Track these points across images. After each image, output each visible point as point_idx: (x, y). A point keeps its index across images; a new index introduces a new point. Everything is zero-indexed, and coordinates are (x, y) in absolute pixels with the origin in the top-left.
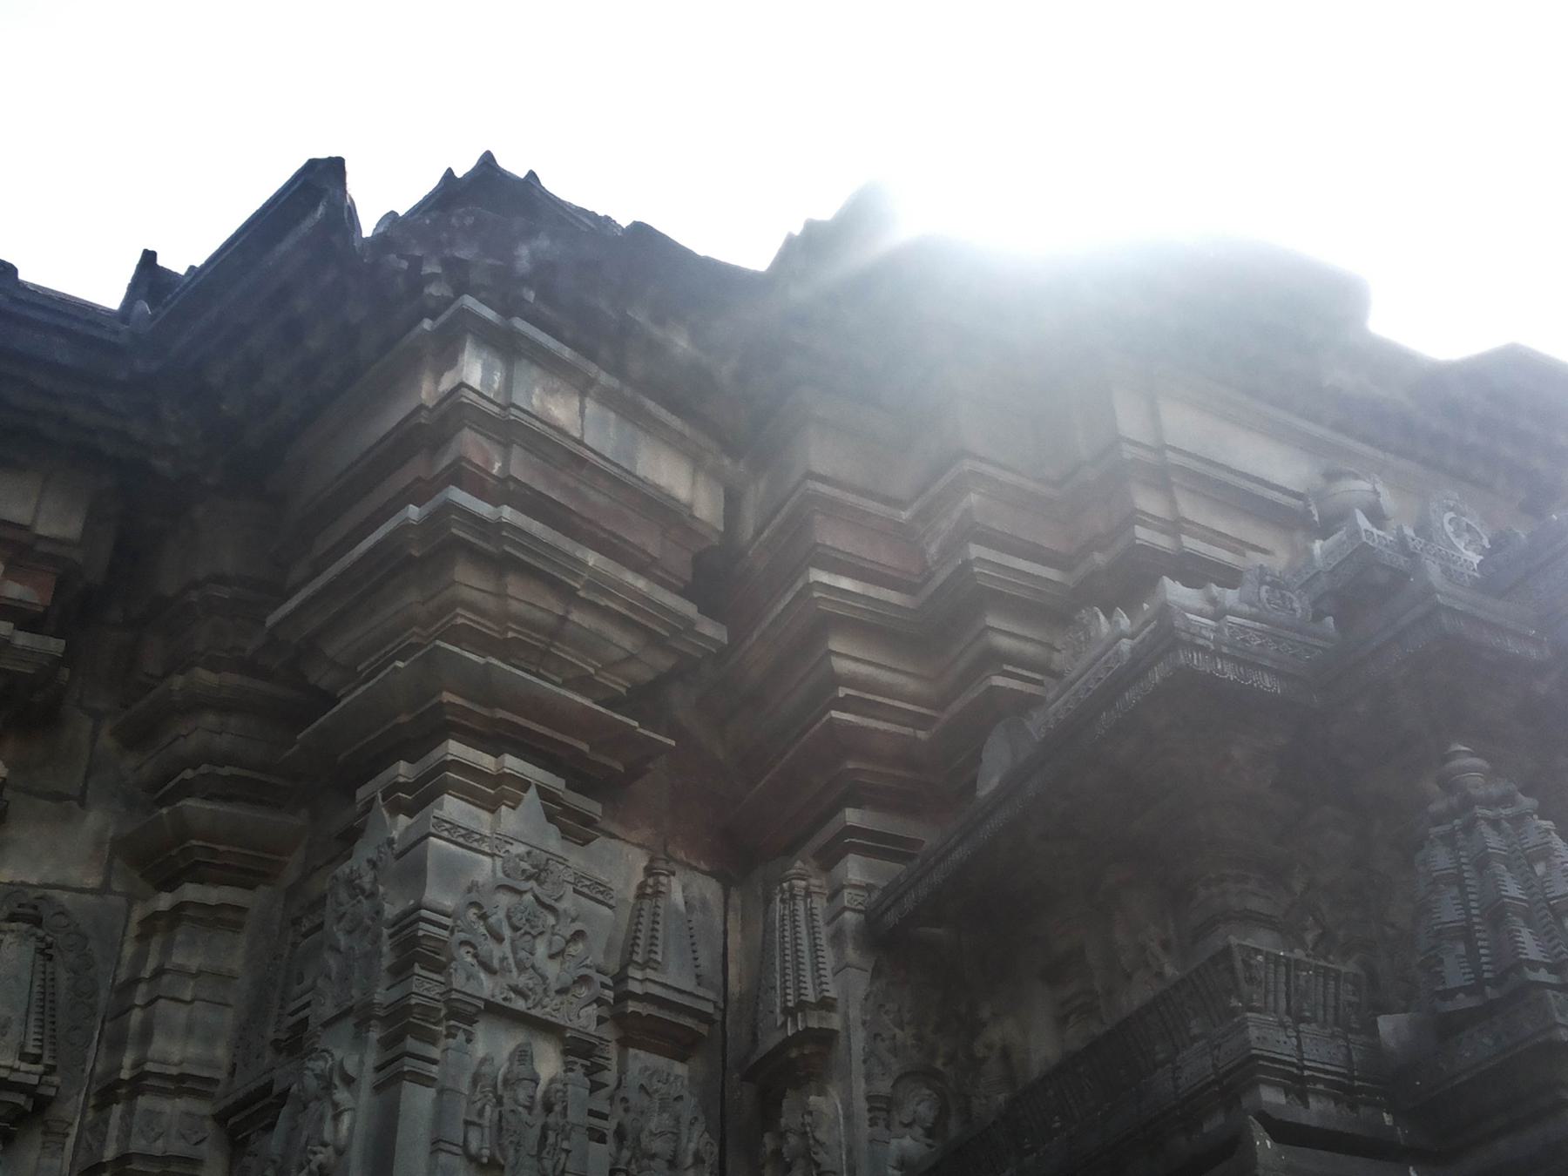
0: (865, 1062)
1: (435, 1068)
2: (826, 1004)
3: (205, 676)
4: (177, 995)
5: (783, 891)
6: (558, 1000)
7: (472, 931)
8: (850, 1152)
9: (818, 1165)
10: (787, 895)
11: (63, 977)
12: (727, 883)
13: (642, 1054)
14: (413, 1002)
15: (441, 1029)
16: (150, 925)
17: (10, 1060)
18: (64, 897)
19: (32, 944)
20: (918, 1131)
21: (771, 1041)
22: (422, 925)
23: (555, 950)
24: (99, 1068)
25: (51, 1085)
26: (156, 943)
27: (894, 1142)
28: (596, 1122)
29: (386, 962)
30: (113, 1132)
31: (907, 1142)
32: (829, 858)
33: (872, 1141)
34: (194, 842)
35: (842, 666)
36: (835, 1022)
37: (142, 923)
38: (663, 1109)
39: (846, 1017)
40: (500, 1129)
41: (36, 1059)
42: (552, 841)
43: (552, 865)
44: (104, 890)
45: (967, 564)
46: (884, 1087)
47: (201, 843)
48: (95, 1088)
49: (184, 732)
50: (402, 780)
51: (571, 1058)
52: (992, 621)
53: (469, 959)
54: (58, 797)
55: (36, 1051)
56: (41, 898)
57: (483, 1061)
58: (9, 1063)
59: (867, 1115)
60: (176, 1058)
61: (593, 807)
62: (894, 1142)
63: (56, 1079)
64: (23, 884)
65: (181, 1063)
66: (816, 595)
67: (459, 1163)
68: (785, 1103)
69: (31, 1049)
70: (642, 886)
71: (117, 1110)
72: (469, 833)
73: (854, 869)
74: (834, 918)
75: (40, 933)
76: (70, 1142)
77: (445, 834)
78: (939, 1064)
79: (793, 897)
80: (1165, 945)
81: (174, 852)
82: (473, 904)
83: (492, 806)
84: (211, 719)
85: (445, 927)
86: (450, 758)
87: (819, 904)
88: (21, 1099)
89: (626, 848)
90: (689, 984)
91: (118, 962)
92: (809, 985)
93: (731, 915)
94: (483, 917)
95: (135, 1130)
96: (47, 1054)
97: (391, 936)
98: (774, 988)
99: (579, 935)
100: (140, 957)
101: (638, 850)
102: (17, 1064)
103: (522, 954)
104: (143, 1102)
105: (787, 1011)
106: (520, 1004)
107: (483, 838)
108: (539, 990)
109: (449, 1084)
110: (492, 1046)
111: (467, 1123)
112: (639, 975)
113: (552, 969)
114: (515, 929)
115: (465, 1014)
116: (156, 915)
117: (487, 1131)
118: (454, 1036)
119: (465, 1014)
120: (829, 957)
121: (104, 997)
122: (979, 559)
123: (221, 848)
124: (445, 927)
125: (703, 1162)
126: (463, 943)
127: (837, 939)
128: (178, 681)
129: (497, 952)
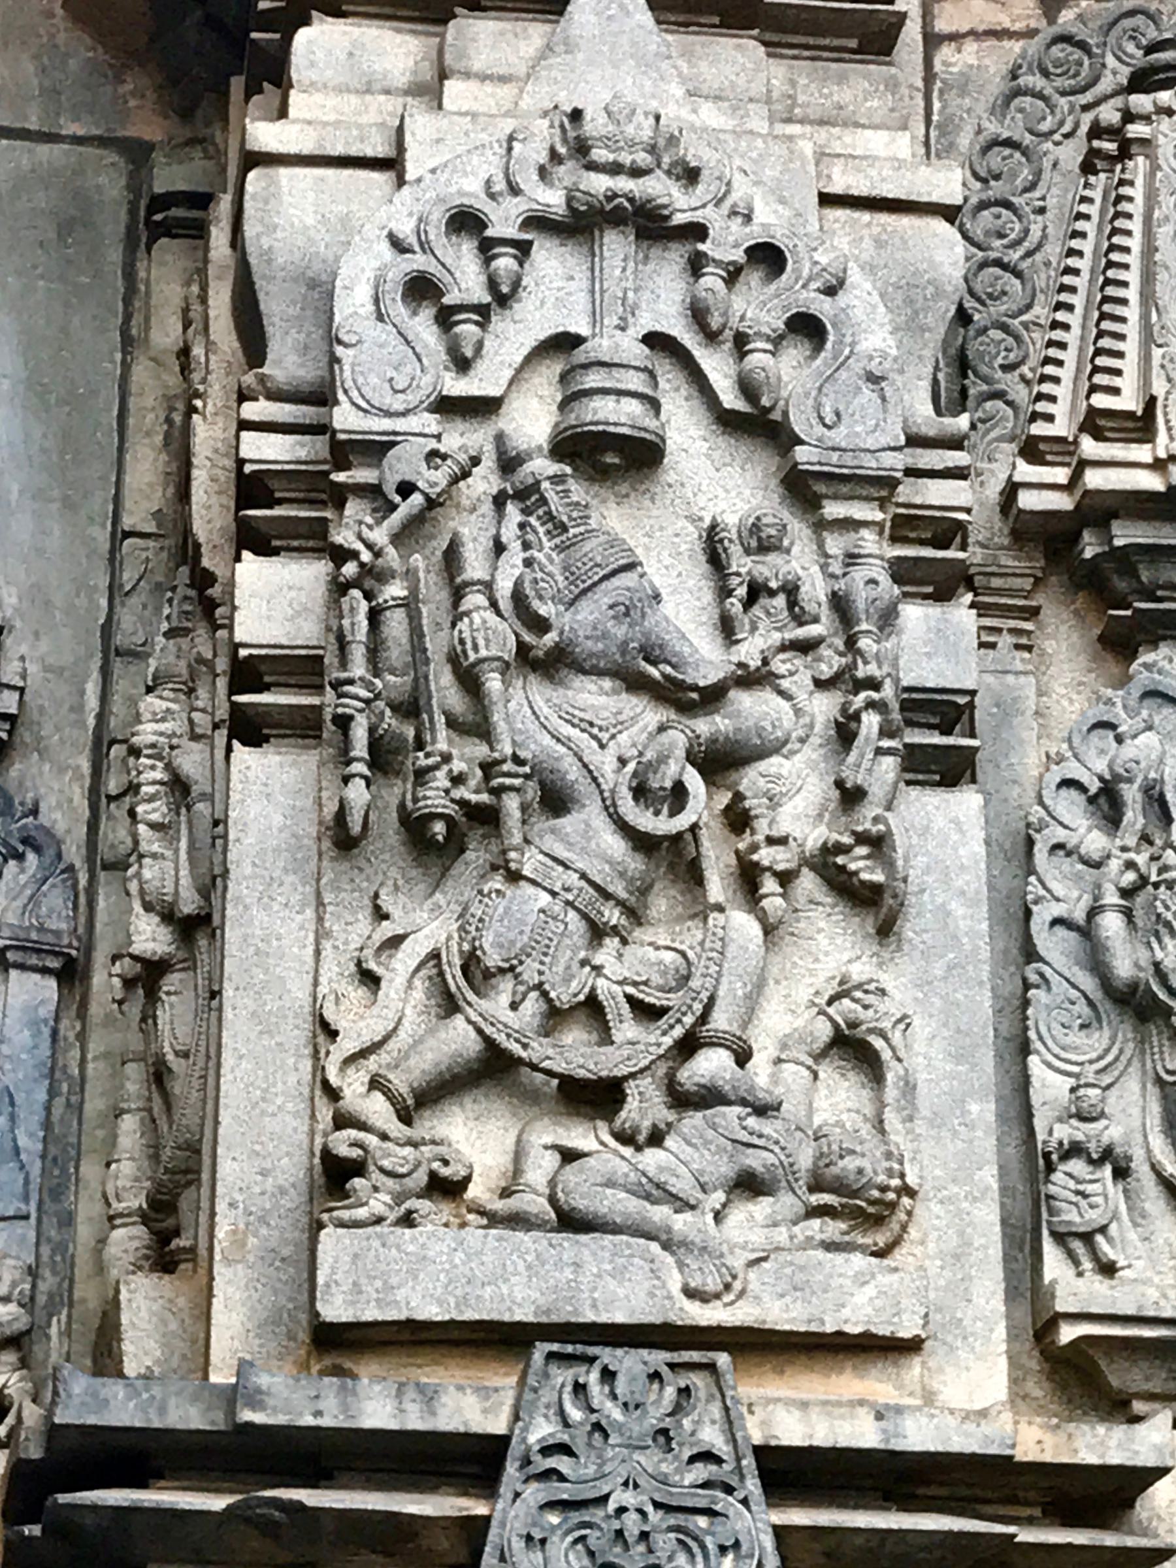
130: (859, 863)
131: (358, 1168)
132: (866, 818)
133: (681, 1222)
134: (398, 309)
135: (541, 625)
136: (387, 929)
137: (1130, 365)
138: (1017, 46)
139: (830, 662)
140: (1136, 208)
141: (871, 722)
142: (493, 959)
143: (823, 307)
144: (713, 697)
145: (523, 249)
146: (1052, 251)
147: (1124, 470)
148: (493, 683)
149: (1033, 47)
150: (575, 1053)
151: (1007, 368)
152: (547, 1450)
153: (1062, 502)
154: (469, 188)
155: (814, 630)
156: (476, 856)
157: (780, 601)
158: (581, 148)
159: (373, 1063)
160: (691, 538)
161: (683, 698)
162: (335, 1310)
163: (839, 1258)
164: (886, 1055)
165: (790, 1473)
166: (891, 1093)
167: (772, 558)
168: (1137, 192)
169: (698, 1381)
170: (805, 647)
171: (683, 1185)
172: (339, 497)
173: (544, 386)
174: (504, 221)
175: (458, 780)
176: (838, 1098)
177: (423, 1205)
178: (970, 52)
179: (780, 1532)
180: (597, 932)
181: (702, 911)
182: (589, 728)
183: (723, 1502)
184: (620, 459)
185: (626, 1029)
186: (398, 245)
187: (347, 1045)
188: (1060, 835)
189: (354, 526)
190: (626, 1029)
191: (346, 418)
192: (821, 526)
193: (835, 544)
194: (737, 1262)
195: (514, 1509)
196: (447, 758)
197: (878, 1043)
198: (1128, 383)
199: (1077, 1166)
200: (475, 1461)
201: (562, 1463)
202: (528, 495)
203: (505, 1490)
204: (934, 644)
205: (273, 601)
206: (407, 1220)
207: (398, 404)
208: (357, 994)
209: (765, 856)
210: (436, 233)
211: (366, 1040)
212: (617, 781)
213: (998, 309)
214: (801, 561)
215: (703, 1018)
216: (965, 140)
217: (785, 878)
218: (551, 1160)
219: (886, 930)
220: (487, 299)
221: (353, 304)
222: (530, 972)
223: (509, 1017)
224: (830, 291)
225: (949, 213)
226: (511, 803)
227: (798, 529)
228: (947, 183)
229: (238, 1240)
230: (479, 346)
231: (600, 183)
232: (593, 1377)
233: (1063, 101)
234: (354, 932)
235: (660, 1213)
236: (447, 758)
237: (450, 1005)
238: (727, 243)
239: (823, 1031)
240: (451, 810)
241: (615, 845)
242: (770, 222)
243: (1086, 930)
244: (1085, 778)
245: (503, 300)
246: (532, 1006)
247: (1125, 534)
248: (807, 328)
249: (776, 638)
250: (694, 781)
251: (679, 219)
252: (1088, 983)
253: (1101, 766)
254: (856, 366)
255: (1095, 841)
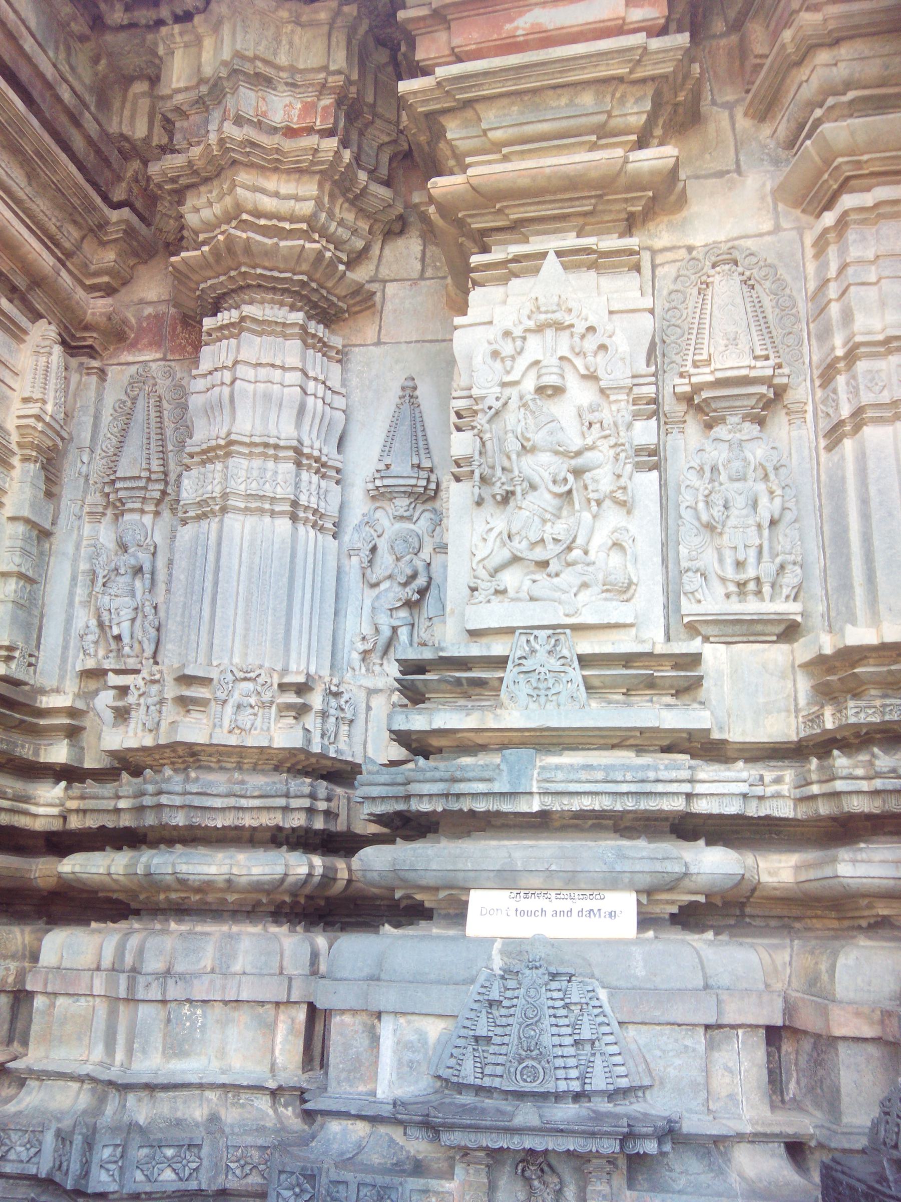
3: (808, 19)
4: (864, 280)
11: (767, 302)
16: (821, 244)
17: (748, 361)
18: (749, 243)
19: (737, 278)
24: (815, 358)
25: (783, 375)
26: (832, 252)
30: (843, 395)
34: (840, 160)
37: (815, 244)
41: (767, 358)
44: (777, 229)
47: (846, 159)
48: (816, 373)
49: (804, 78)
54: (721, 174)
55: (764, 353)
56: (732, 248)
58: (746, 363)
60: (878, 326)
63: (786, 370)
64: (714, 242)
65: (883, 330)
69: (759, 352)
71: (841, 380)
75: (740, 269)
76: (809, 416)
81: (826, 176)
84: (823, 56)
88: (763, 389)
91: (805, 279)
95: (862, 387)
96: (772, 356)
100: (823, 266)
102: (753, 363)
104: (861, 366)
116: (826, 231)
121: (803, 307)
123: (865, 157)
128: (787, 35)
130: (619, 495)
131: (476, 589)
132: (622, 482)
133: (564, 597)
134: (489, 360)
135: (528, 440)
136: (489, 526)
137: (705, 347)
138: (678, 264)
139: (612, 441)
140: (709, 302)
141: (623, 455)
142: (514, 531)
143: (607, 342)
144: (578, 454)
145: (524, 338)
146: (690, 319)
147: (704, 376)
148: (514, 457)
149: (683, 263)
150: (539, 554)
151: (677, 354)
152: (520, 658)
153: (688, 389)
154: (508, 324)
155: (608, 432)
156: (512, 503)
157: (598, 425)
158: (538, 308)
159: (485, 562)
160: (574, 412)
161: (565, 454)
162: (471, 626)
163: (608, 603)
164: (627, 547)
165: (585, 661)
166: (628, 557)
167: (596, 414)
168: (709, 297)
169: (562, 637)
170: (605, 437)
171: (565, 586)
172: (476, 412)
173: (533, 374)
174: (518, 332)
175: (503, 484)
176: (615, 559)
177: (493, 597)
178: (667, 268)
179: (584, 677)
180: (544, 521)
181: (573, 512)
182: (541, 466)
183: (567, 669)
184: (550, 391)
185: (550, 545)
186: (490, 343)
187: (478, 558)
188: (688, 483)
189: (481, 420)
190: (550, 545)
191: (475, 392)
192: (610, 403)
193: (614, 407)
194: (579, 606)
195: (510, 673)
196: (500, 478)
197: (624, 544)
198: (705, 352)
199: (690, 574)
200: (501, 662)
201: (523, 661)
202: (525, 405)
203: (508, 669)
204: (645, 432)
205: (461, 444)
206: (489, 601)
207: (489, 385)
208: (481, 544)
209: (592, 495)
210: (499, 338)
211: (484, 556)
212: (548, 479)
213: (672, 338)
214: (606, 415)
215: (574, 541)
216: (665, 292)
217: (599, 503)
218: (530, 582)
219: (629, 512)
220: (513, 352)
221: (478, 360)
222: (523, 534)
223: (518, 546)
224: (610, 336)
225: (652, 311)
226: (518, 490)
227: (605, 405)
228: (648, 303)
229: (453, 612)
230: (512, 367)
231: (542, 317)
232: (532, 638)
233: (693, 277)
234: (481, 528)
235: (557, 595)
236: (500, 478)
237: (504, 544)
238: (580, 328)
239: (610, 543)
240: (501, 492)
241: (548, 496)
242: (592, 321)
243: (695, 509)
244: (696, 466)
245: (519, 353)
246: (525, 543)
247: (705, 395)
248: (603, 347)
249: (598, 435)
250: (570, 478)
251: (566, 324)
252: (697, 524)
253: (698, 461)
254: (618, 356)
255: (697, 483)
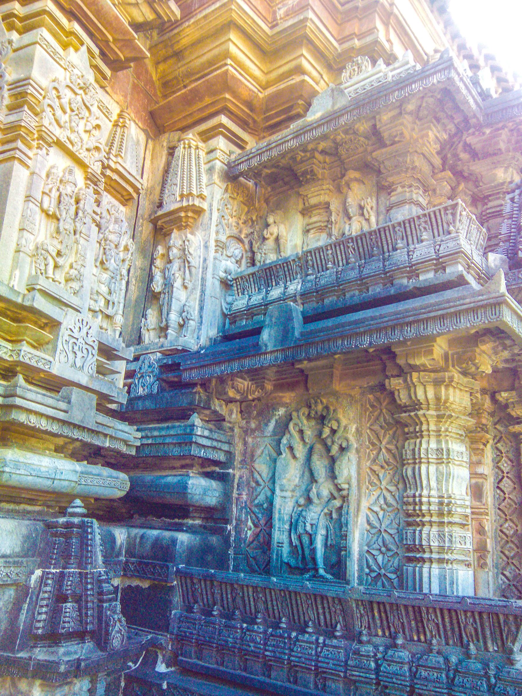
0: (217, 226)
1: (29, 161)
2: (201, 197)
5: (184, 144)
6: (86, 153)
7: (55, 103)
8: (205, 260)
9: (189, 262)
10: (187, 146)
12: (148, 137)
13: (109, 196)
14: (23, 124)
15: (35, 143)
20: (233, 260)
21: (170, 206)
22: (30, 87)
23: (88, 128)
27: (224, 262)
28: (94, 215)
29: (7, 101)
31: (229, 263)
32: (206, 136)
33: (215, 259)
35: (233, 49)
36: (205, 206)
38: (116, 222)
39: (211, 205)
40: (60, 202)
42: (90, 77)
43: (91, 88)
45: (306, 19)
46: (223, 238)
50: (16, 12)
51: (89, 182)
52: (305, 52)
53: (51, 114)
57: (52, 167)
59: (214, 248)
61: (108, 72)
62: (224, 262)
66: (233, 7)
67: (38, 210)
68: (173, 235)
70: (116, 121)
72: (56, 53)
73: (221, 143)
74: (209, 162)
77: (45, 46)
78: (243, 236)
79: (190, 147)
80: (372, 208)
82: (55, 88)
83: (65, 46)
85: (41, 95)
86: (47, 9)
87: (202, 154)
89: (112, 101)
90: (134, 173)
92: (195, 187)
93: (147, 152)
94: (59, 97)
97: (9, 90)
98: (176, 185)
99: (98, 127)
101: (116, 105)
103: (73, 124)
105: (182, 196)
106: (70, 146)
107: (61, 58)
108: (80, 144)
109: (37, 171)
110: (57, 161)
111: (44, 193)
112: (114, 159)
113: (85, 136)
114: (72, 111)
115: (46, 140)
117: (53, 200)
118: (41, 149)
119: (46, 140)
120: (204, 178)
122: (311, 20)
124: (41, 95)
125: (128, 250)
126: (49, 106)
127: (211, 170)
129: (64, 118)
